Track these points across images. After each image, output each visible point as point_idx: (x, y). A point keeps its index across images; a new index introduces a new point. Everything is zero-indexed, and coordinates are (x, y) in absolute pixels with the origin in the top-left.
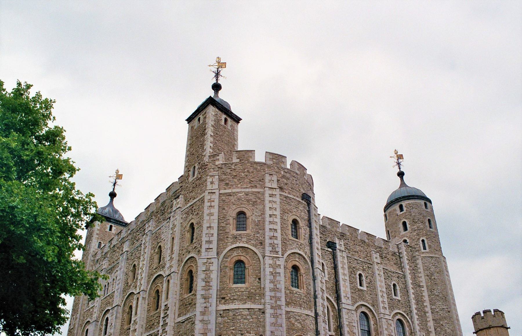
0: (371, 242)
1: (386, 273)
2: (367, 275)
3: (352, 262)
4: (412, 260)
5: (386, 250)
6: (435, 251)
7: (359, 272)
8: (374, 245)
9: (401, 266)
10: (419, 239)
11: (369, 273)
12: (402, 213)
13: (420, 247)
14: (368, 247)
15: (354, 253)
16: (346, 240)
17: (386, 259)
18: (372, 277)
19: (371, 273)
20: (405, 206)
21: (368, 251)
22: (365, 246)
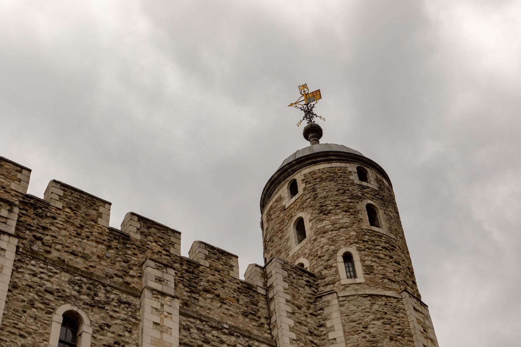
0: (156, 242)
1: (198, 329)
2: (109, 321)
3: (43, 276)
4: (309, 308)
5: (216, 273)
6: (386, 281)
7: (67, 307)
8: (164, 252)
9: (269, 324)
10: (335, 252)
11: (118, 318)
12: (294, 199)
13: (337, 272)
14: (136, 252)
15: (72, 257)
16: (42, 217)
17: (209, 296)
18: (130, 332)
19: (125, 320)
20: (303, 180)
21: (132, 262)
22: (129, 248)
